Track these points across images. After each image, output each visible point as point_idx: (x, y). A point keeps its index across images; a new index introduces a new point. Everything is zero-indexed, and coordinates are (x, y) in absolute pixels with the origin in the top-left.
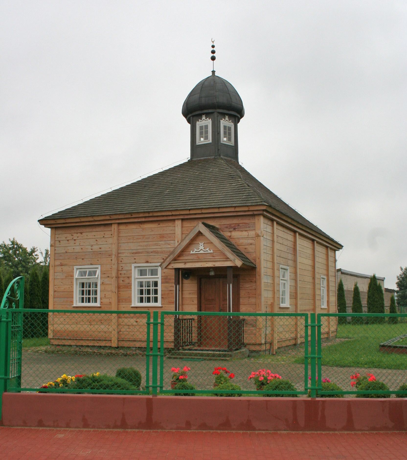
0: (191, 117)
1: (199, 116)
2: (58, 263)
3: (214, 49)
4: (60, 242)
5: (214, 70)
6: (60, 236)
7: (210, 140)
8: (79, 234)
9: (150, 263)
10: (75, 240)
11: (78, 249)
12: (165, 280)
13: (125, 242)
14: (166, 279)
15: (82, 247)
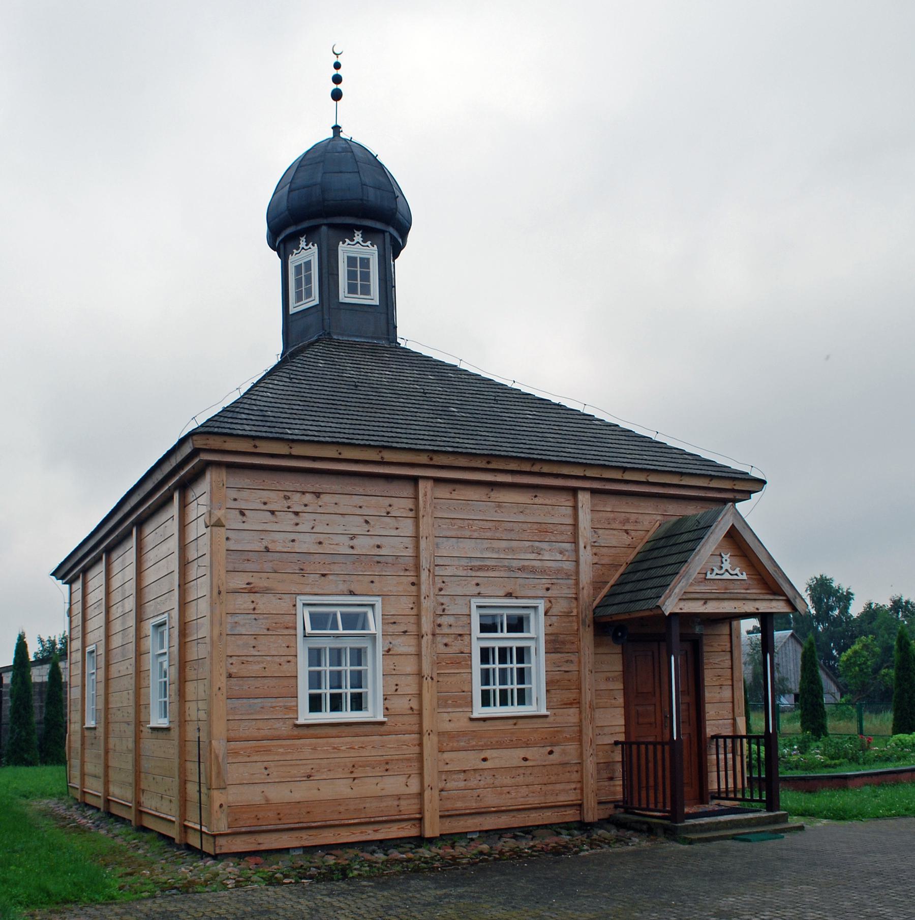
0: (324, 228)
1: (347, 231)
2: (239, 581)
3: (340, 72)
4: (242, 514)
5: (338, 124)
6: (245, 494)
7: (374, 298)
8: (308, 498)
9: (517, 598)
10: (296, 513)
11: (306, 543)
12: (554, 644)
13: (449, 534)
14: (554, 641)
15: (321, 537)
